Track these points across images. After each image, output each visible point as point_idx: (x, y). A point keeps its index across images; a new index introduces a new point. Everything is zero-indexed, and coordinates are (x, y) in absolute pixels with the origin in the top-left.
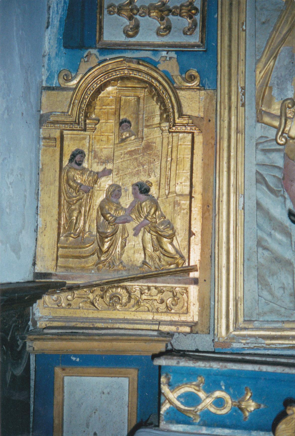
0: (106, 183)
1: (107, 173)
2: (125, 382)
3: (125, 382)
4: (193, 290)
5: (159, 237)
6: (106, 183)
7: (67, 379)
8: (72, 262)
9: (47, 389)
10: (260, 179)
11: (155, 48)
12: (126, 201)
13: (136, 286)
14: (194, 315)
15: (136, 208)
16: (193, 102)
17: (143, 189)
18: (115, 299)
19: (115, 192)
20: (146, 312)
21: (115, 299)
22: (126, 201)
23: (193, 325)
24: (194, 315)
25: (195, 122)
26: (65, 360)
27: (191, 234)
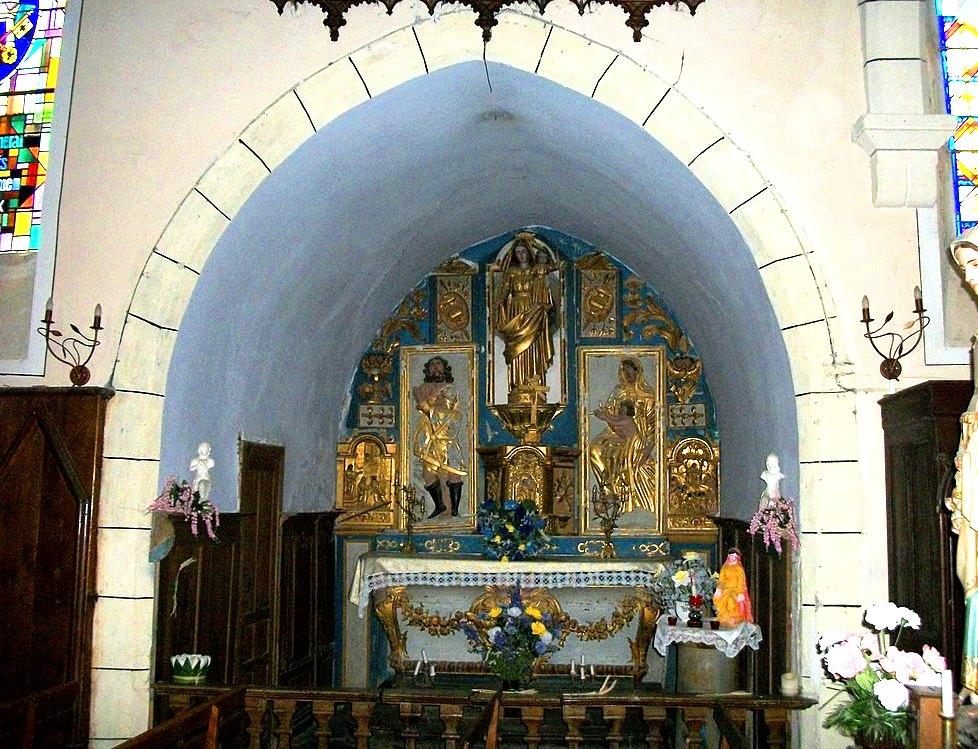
0: (361, 476)
1: (361, 473)
2: (367, 544)
3: (367, 544)
4: (391, 514)
5: (380, 495)
6: (361, 476)
7: (348, 544)
8: (349, 505)
9: (341, 546)
10: (415, 475)
11: (379, 429)
12: (368, 482)
13: (371, 513)
14: (392, 523)
15: (371, 484)
16: (391, 448)
17: (374, 478)
18: (364, 518)
19: (363, 480)
20: (375, 521)
21: (364, 518)
22: (368, 482)
23: (391, 526)
24: (392, 523)
25: (392, 455)
26: (346, 537)
27: (391, 494)
